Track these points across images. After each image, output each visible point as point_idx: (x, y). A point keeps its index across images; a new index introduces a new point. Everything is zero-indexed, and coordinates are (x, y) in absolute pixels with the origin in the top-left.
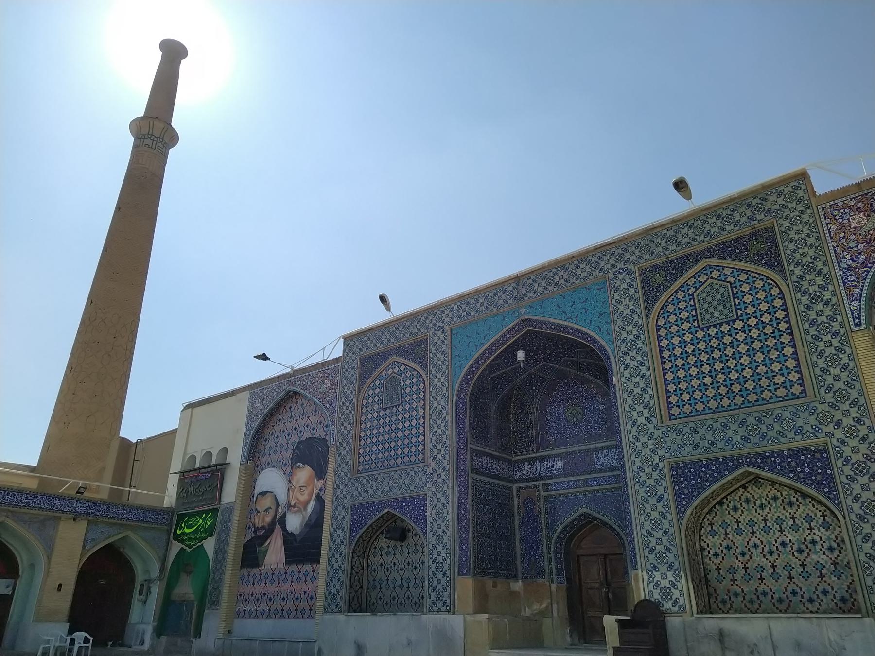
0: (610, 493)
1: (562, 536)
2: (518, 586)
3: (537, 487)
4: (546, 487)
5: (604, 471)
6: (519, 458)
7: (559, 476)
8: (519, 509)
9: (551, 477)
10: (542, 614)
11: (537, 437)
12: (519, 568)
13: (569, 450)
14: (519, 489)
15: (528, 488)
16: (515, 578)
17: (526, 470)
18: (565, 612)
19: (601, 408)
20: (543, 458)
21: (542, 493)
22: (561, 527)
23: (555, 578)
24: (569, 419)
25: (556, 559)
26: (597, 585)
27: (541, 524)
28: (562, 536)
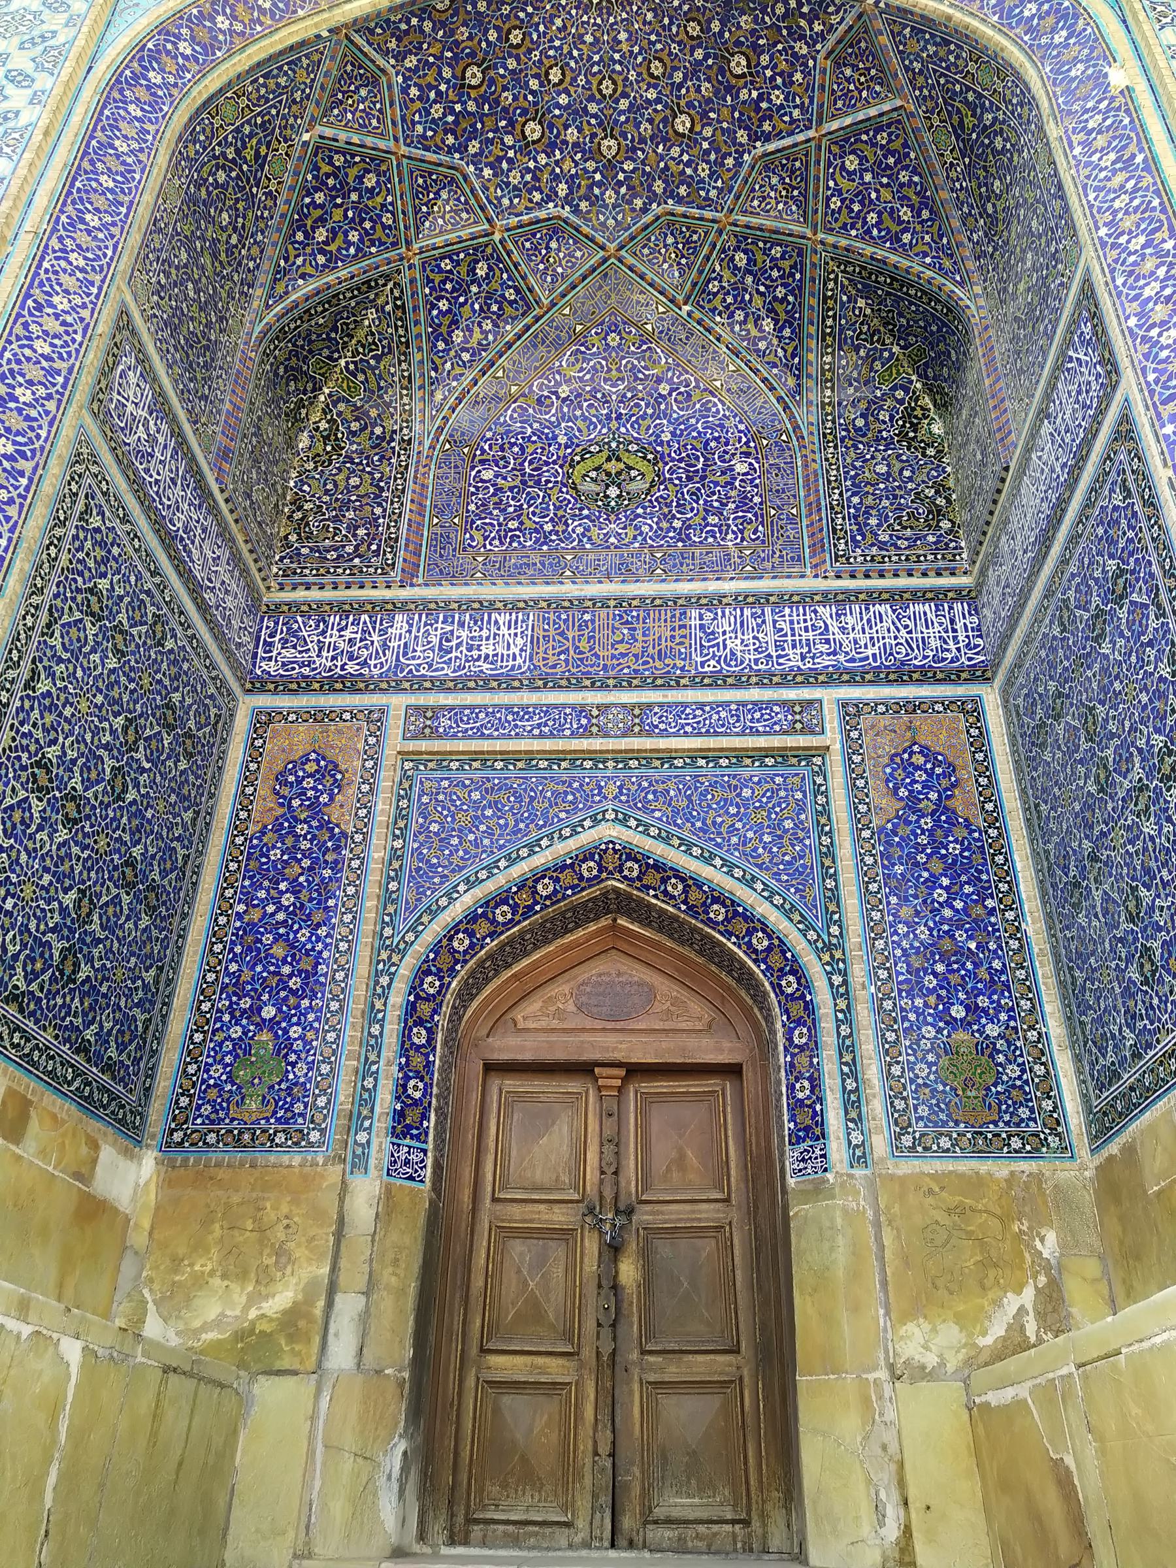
0: (752, 771)
1: (461, 943)
2: (131, 1176)
3: (376, 719)
4: (425, 722)
5: (740, 682)
6: (301, 594)
7: (507, 682)
8: (244, 801)
9: (460, 685)
10: (257, 1351)
11: (416, 527)
12: (165, 1082)
13: (569, 590)
14: (263, 722)
15: (319, 716)
16: (129, 1126)
17: (327, 647)
18: (396, 1352)
19: (741, 468)
20: (427, 608)
21: (394, 740)
22: (467, 900)
23: (380, 1144)
24: (588, 487)
25: (406, 1046)
26: (560, 1217)
27: (360, 874)
28: (461, 943)
